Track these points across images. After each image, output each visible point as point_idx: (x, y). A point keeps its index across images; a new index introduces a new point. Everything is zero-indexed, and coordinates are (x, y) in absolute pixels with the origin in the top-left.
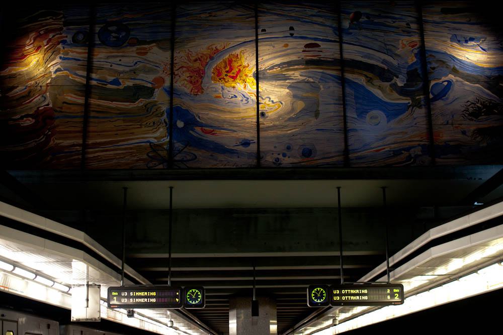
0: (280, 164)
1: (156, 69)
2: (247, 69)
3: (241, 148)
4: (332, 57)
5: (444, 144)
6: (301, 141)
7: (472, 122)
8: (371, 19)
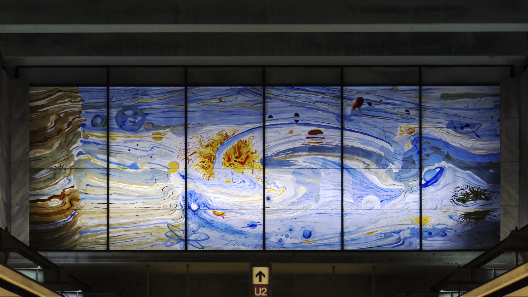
0: (283, 244)
1: (171, 154)
2: (255, 155)
3: (249, 229)
4: (333, 144)
5: (432, 227)
6: (301, 223)
7: (459, 207)
8: (373, 105)
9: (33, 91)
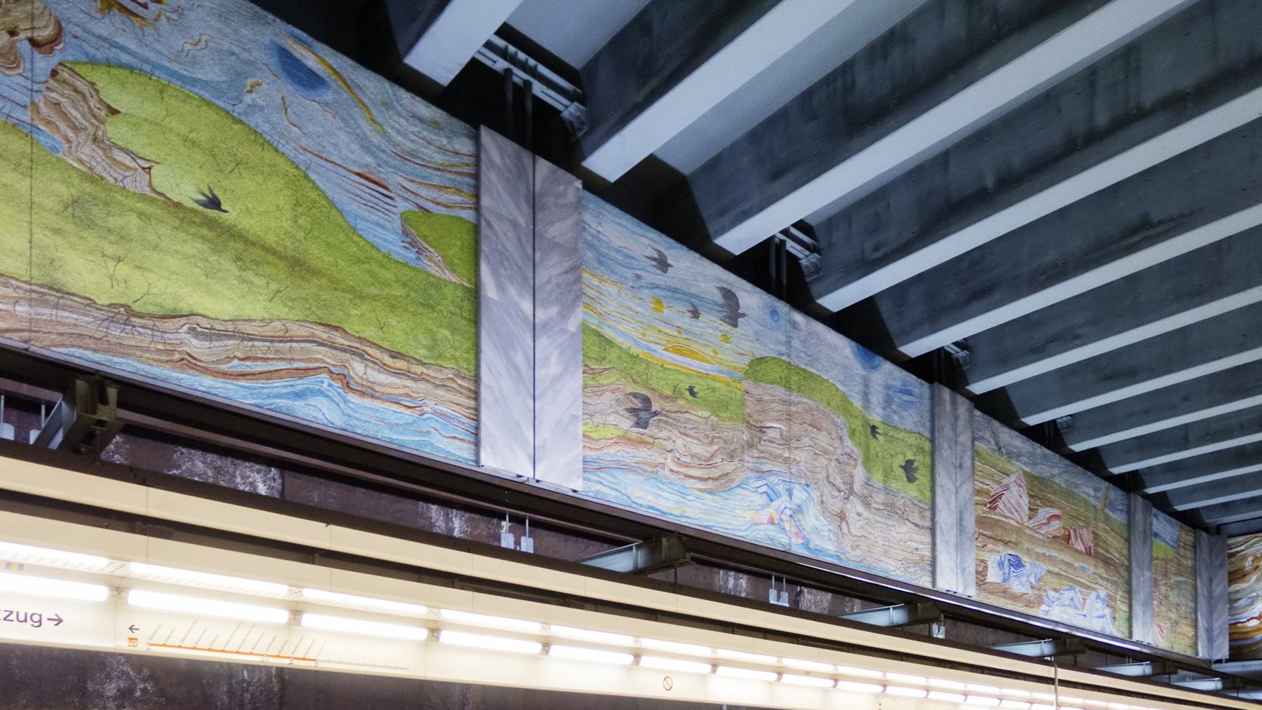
9: (1231, 541)
